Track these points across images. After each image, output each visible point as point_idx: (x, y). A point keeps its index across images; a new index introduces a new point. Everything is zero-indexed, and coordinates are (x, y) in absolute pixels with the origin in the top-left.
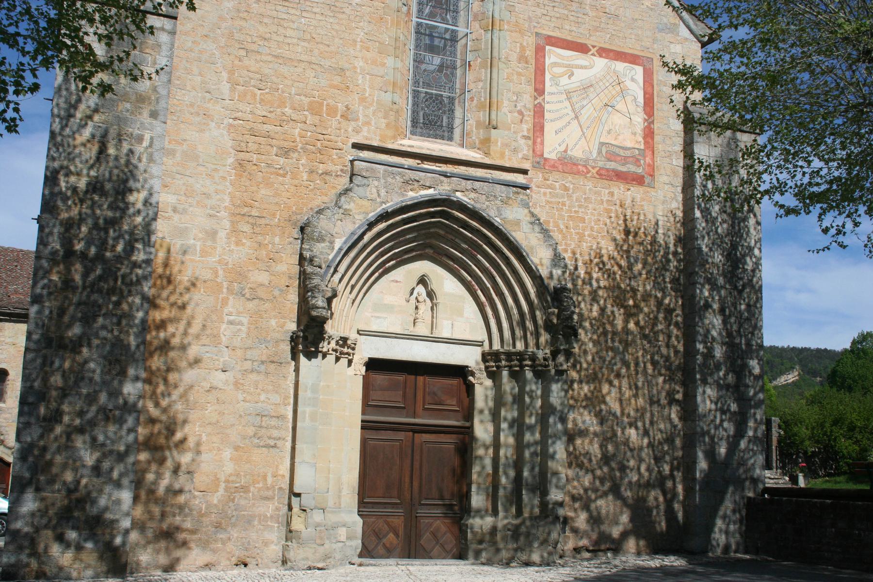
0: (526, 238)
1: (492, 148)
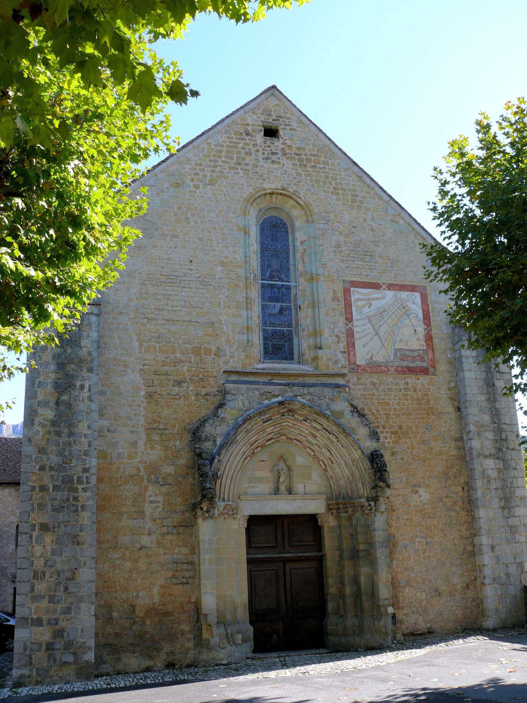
0: (349, 422)
1: (319, 363)
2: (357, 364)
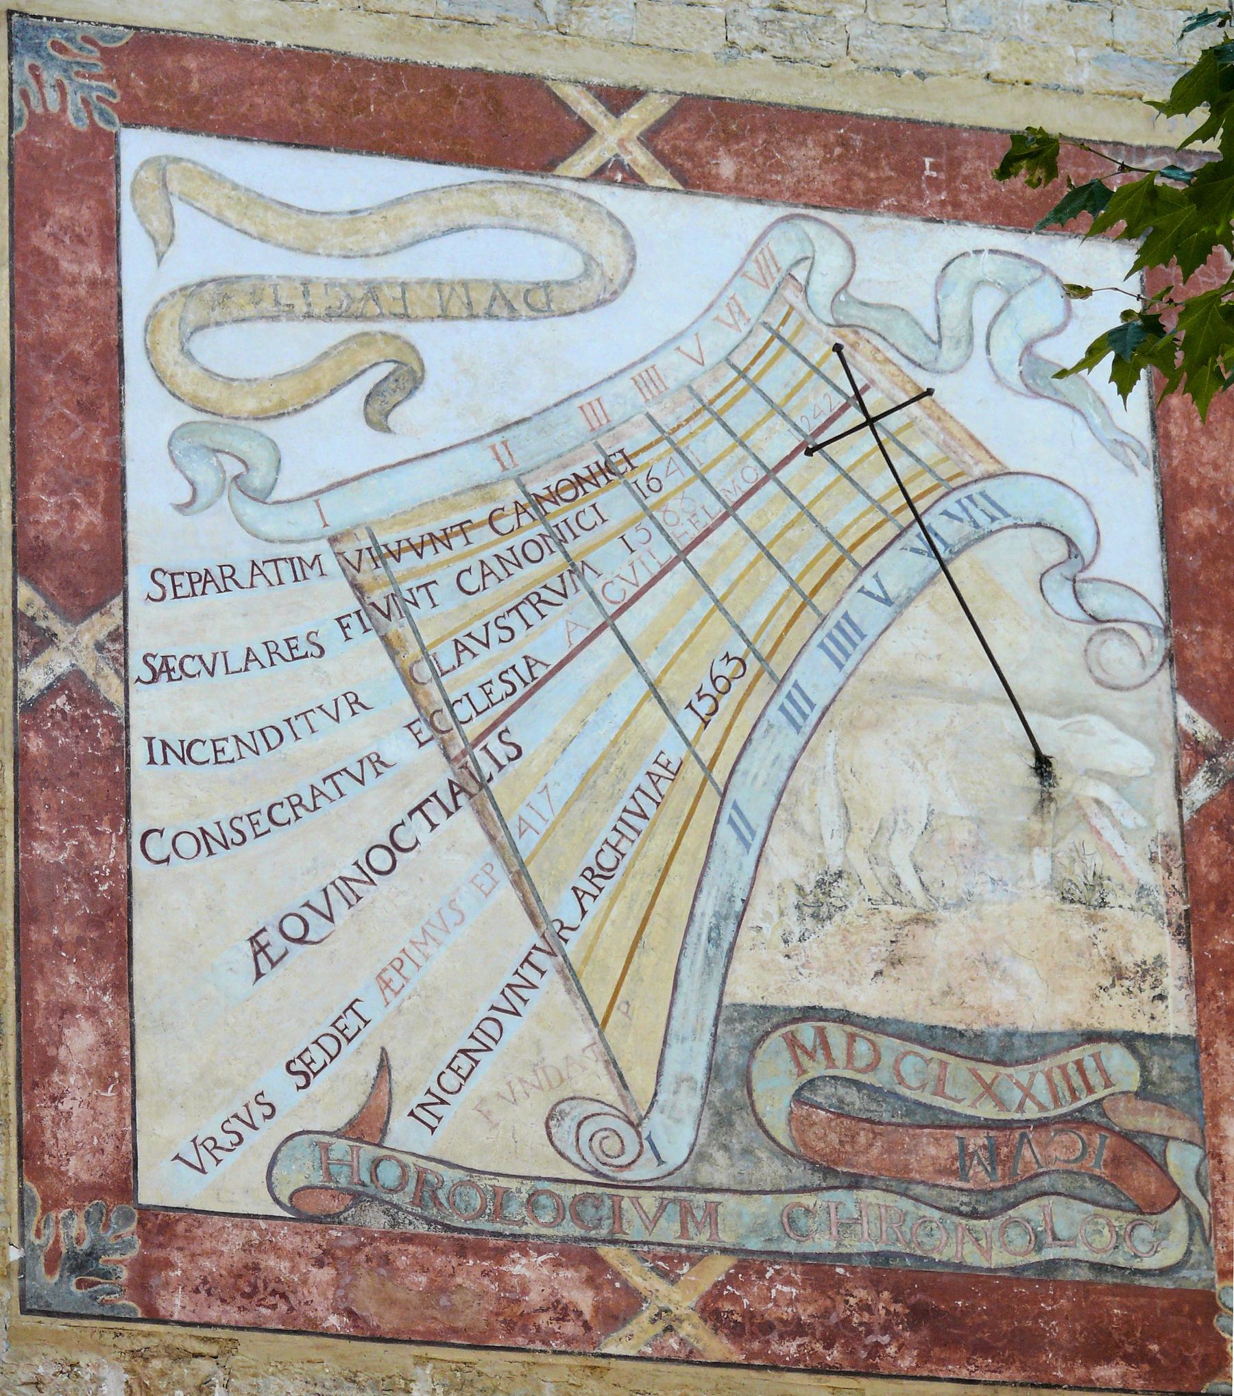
2: (148, 1195)
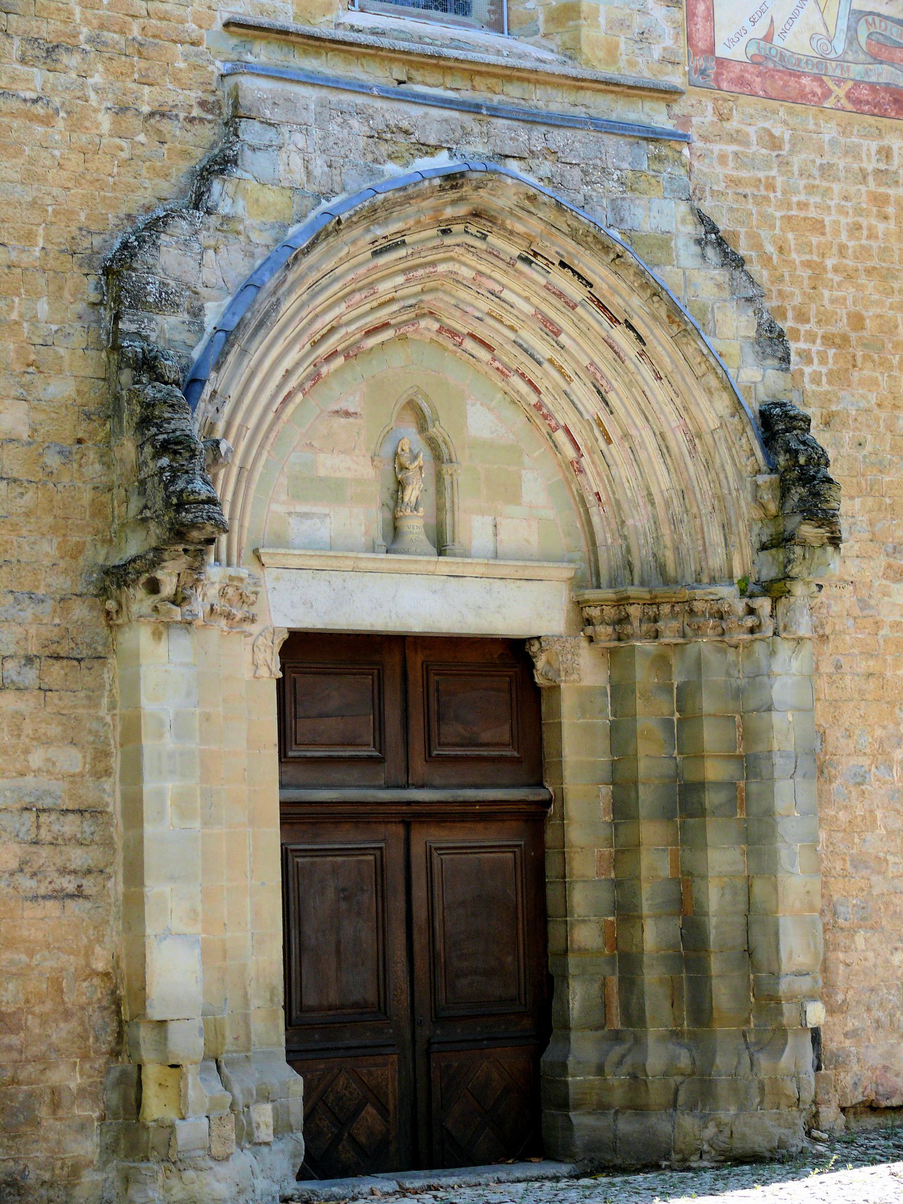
0: (687, 282)
1: (584, 32)
2: (718, 54)
